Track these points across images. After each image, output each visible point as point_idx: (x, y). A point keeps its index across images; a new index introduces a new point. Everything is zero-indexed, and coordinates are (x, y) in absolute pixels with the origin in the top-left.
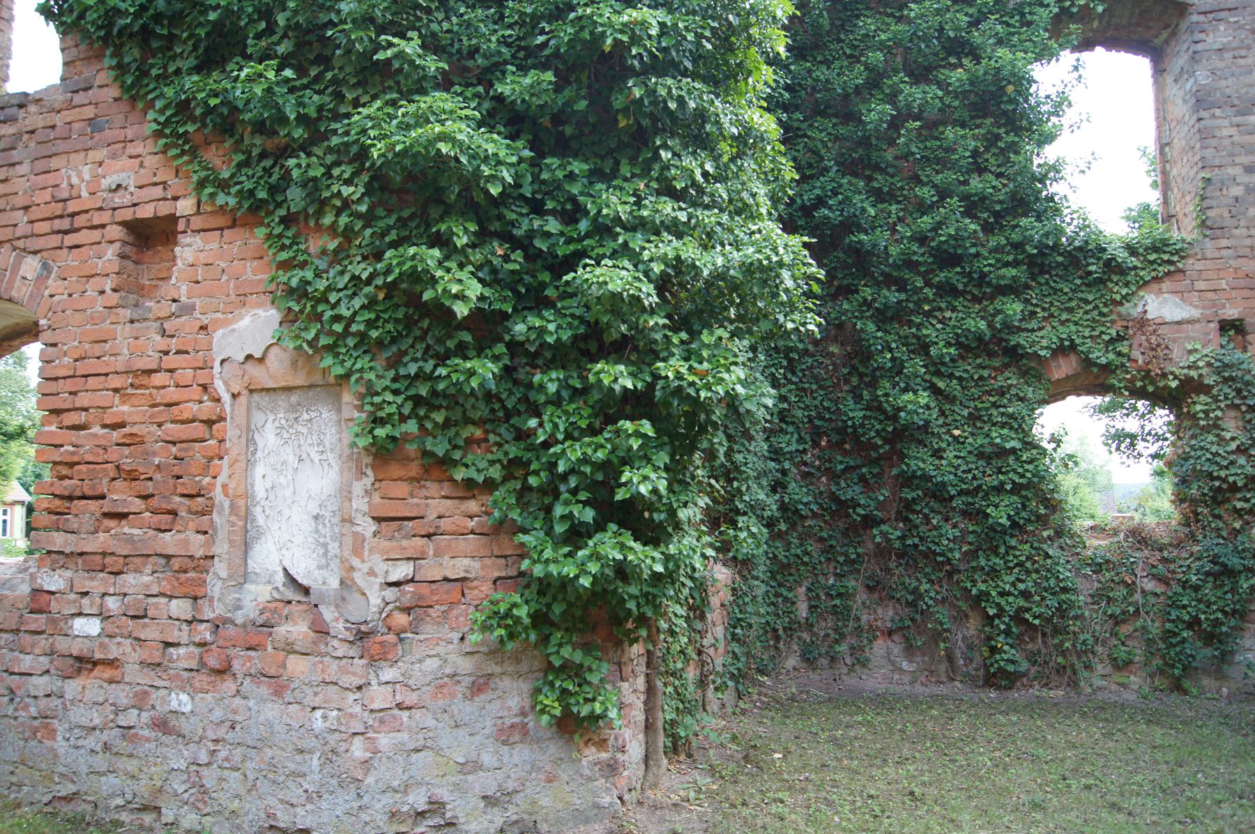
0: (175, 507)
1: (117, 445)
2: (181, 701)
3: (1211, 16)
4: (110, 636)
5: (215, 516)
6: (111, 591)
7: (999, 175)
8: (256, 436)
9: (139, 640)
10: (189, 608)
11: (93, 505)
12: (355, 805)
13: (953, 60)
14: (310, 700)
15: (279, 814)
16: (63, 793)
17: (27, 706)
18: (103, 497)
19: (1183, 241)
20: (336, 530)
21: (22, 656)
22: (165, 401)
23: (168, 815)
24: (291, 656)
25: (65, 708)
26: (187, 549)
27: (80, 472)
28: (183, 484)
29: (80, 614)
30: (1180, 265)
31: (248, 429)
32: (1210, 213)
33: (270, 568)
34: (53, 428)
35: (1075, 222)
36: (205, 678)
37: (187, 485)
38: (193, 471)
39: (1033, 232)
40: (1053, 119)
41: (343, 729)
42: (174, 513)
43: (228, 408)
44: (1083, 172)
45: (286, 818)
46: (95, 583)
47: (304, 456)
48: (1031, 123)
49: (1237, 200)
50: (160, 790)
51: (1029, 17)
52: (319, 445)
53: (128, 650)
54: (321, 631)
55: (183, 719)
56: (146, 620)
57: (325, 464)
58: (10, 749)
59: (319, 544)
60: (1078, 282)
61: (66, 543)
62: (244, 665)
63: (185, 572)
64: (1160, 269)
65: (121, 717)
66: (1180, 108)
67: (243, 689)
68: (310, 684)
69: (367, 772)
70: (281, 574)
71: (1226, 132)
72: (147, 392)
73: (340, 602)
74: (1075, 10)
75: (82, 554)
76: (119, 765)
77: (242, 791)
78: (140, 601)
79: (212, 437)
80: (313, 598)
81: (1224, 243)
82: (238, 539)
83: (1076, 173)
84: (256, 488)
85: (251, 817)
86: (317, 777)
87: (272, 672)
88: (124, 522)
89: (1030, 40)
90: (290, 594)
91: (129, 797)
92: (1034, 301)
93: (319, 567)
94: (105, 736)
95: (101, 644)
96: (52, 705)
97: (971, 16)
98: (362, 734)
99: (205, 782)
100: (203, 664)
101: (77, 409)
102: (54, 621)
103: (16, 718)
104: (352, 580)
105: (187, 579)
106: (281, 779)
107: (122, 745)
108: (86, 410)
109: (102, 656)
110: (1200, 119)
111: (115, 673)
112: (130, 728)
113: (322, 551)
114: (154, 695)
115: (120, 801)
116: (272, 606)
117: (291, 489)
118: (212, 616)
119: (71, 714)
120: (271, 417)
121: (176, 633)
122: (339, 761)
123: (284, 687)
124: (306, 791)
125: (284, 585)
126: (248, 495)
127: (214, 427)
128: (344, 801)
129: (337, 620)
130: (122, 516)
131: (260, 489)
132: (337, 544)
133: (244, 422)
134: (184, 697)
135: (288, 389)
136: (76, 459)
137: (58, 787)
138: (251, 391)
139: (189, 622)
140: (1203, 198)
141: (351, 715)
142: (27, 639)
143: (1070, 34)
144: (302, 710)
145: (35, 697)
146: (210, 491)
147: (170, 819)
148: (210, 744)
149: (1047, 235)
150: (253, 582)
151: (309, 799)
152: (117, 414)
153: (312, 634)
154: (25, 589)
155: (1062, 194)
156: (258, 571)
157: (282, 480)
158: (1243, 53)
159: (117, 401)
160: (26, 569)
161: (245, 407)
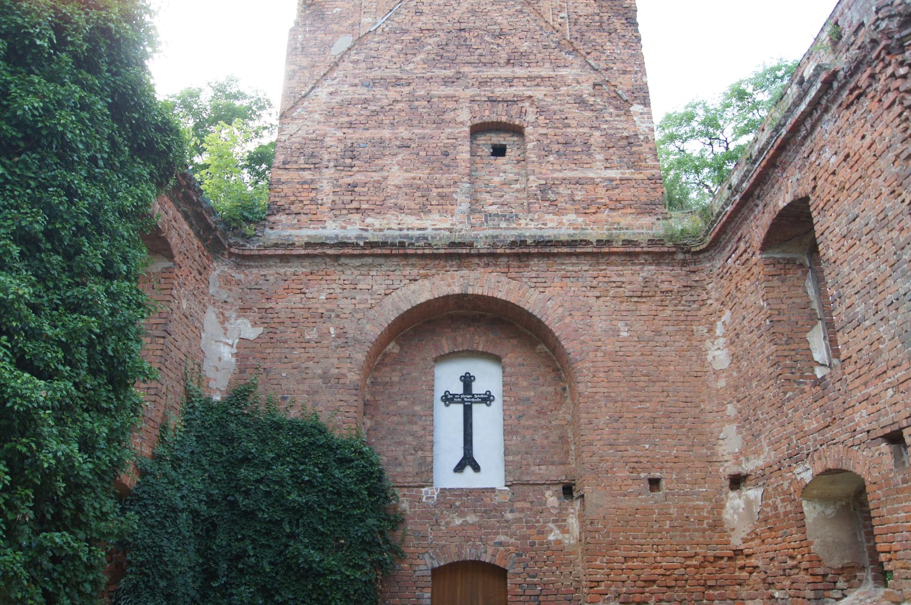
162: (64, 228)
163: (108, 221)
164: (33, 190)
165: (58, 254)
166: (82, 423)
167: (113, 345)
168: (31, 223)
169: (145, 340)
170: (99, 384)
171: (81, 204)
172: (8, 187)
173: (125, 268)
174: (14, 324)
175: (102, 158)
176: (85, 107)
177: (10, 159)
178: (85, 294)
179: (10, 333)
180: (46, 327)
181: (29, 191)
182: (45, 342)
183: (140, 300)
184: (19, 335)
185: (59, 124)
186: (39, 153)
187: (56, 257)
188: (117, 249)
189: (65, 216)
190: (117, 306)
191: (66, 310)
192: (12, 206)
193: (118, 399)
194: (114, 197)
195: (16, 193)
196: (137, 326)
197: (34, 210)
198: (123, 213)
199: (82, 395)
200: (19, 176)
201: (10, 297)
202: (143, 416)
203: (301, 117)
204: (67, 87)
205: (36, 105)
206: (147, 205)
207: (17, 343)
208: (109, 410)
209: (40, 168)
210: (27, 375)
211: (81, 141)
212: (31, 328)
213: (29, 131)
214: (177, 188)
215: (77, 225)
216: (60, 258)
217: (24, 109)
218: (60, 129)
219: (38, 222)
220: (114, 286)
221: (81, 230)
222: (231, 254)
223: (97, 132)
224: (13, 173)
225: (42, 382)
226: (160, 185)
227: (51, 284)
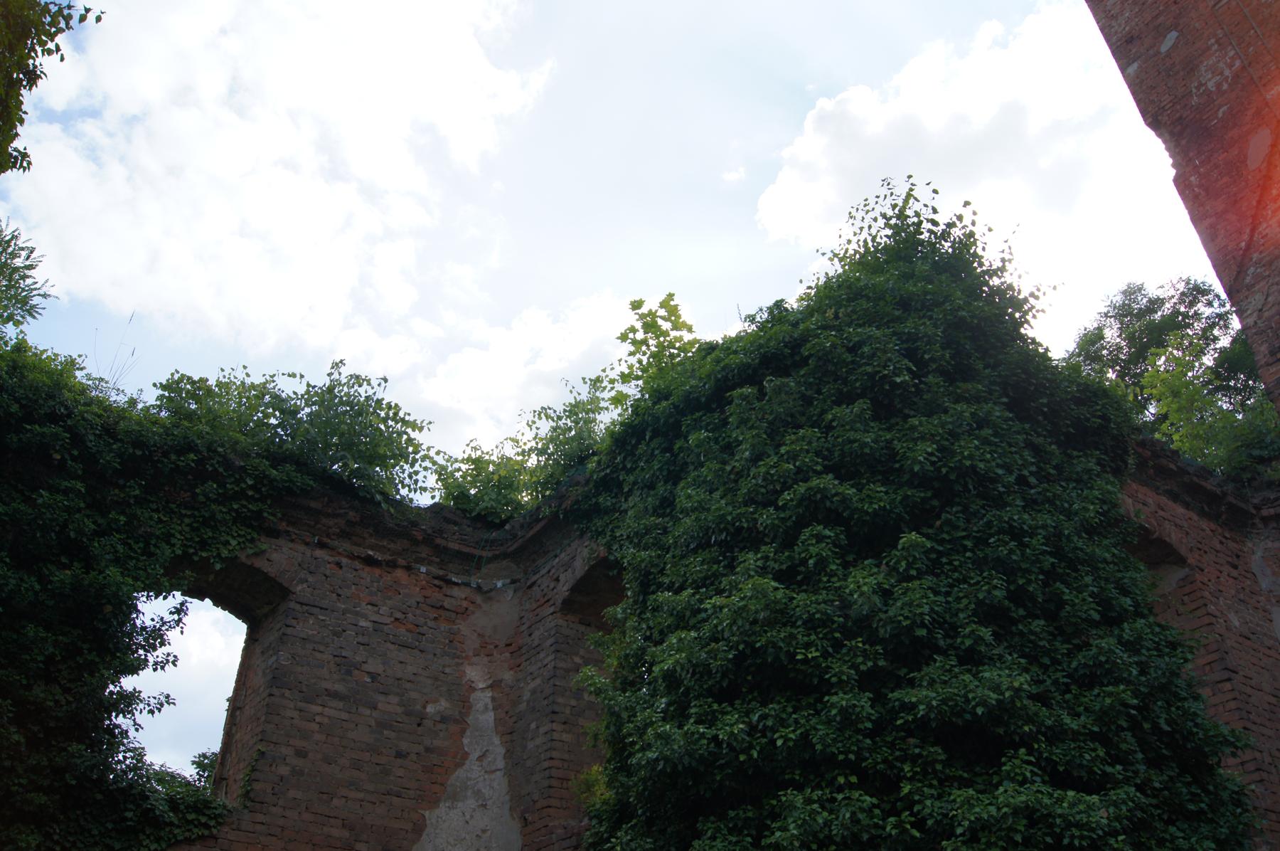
3: (306, 608)
7: (66, 691)
13: (64, 560)
19: (225, 807)
30: (215, 831)
32: (257, 786)
35: (128, 762)
39: (79, 761)
40: (141, 652)
44: (151, 712)
48: (118, 649)
49: (282, 778)
51: (152, 549)
60: (110, 826)
64: (196, 830)
66: (258, 680)
71: (289, 713)
74: (196, 558)
81: (260, 817)
83: (145, 712)
89: (145, 570)
92: (56, 837)
97: (99, 526)
110: (271, 695)
140: (254, 770)
143: (185, 578)
149: (94, 766)
155: (124, 727)
158: (322, 648)
162: (1029, 582)
163: (1077, 548)
164: (972, 551)
165: (1038, 617)
166: (1172, 841)
167: (1164, 716)
168: (989, 592)
169: (1205, 692)
170: (1171, 778)
171: (1034, 542)
172: (944, 560)
173: (1129, 601)
174: (1026, 728)
175: (1031, 473)
176: (982, 423)
177: (931, 526)
178: (1095, 657)
179: (1026, 741)
180: (1067, 720)
181: (968, 554)
182: (1073, 740)
183: (1170, 638)
184: (1038, 741)
185: (964, 458)
186: (959, 504)
187: (1037, 622)
188: (1107, 580)
189: (1024, 566)
190: (1143, 659)
191: (1080, 687)
192: (958, 580)
193: (1208, 792)
194: (1069, 515)
195: (956, 563)
196: (1184, 676)
197: (985, 574)
198: (1090, 531)
199: (1154, 801)
200: (949, 541)
201: (1007, 694)
202: (1255, 808)
203: (1258, 278)
204: (951, 411)
205: (929, 450)
206: (1115, 506)
207: (1041, 753)
208: (1202, 812)
209: (968, 521)
210: (1071, 793)
211: (998, 466)
212: (1048, 728)
213: (936, 484)
214: (1142, 464)
215: (1042, 572)
216: (1042, 622)
217: (920, 462)
218: (968, 463)
219: (995, 587)
220: (1127, 631)
221: (1051, 576)
222: (1266, 520)
223: (1011, 446)
224: (942, 542)
225: (1095, 798)
226: (1117, 472)
227: (1046, 661)
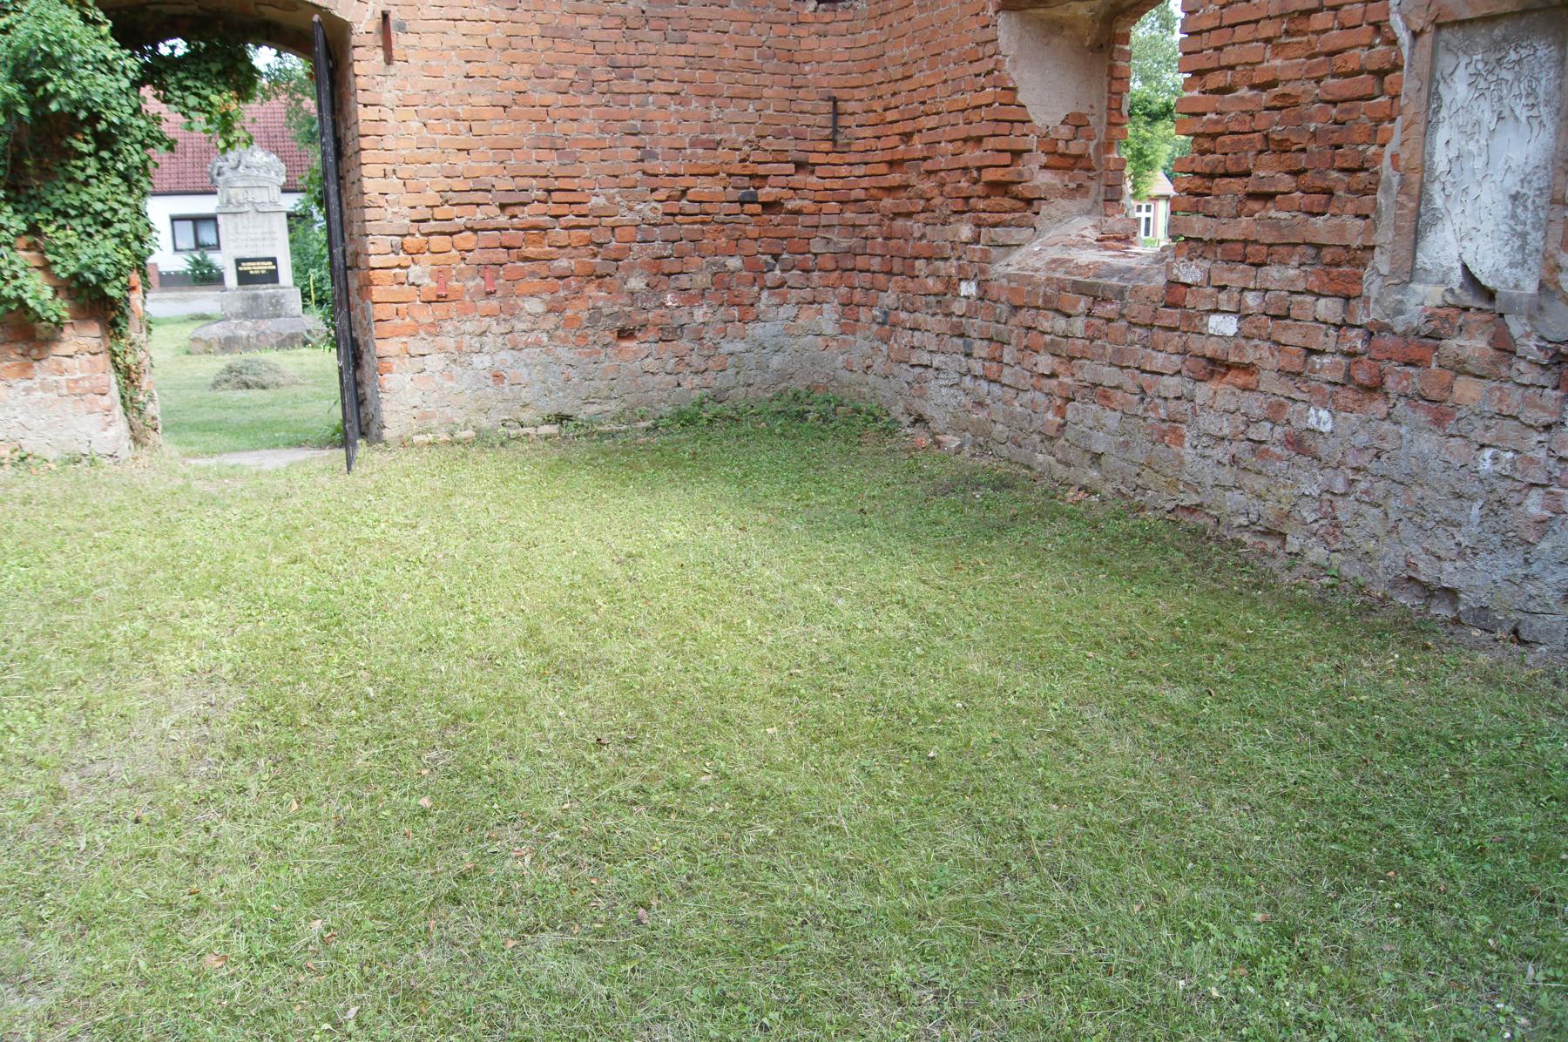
0: (1331, 184)
1: (1267, 109)
2: (1320, 418)
4: (1247, 338)
5: (1380, 196)
6: (1252, 286)
8: (1442, 88)
9: (1277, 343)
10: (1339, 310)
11: (1236, 184)
12: (1520, 572)
14: (1478, 435)
15: (1421, 565)
16: (1186, 503)
17: (1156, 408)
18: (1248, 174)
20: (1542, 215)
21: (1154, 354)
22: (1325, 50)
23: (1294, 544)
24: (1460, 378)
25: (1195, 414)
26: (1342, 237)
27: (1223, 144)
28: (1343, 155)
29: (1216, 311)
31: (1432, 79)
33: (1445, 263)
34: (1195, 93)
36: (1351, 395)
37: (1347, 157)
38: (1356, 137)
41: (1518, 476)
42: (1329, 192)
43: (1405, 52)
45: (1430, 572)
46: (1234, 276)
47: (1506, 113)
50: (1288, 515)
52: (1528, 95)
53: (1266, 354)
54: (1505, 348)
55: (1320, 439)
56: (1288, 322)
57: (1535, 123)
58: (1138, 450)
59: (1514, 233)
61: (1205, 229)
62: (1399, 383)
63: (1338, 265)
65: (1252, 429)
67: (1395, 412)
68: (1481, 416)
69: (1542, 535)
70: (1459, 272)
72: (1305, 39)
73: (1536, 310)
75: (1221, 242)
76: (1246, 481)
77: (1380, 532)
78: (1283, 299)
79: (1382, 93)
80: (1498, 306)
82: (1407, 225)
84: (1436, 159)
85: (1387, 562)
86: (1475, 530)
87: (1434, 395)
88: (1270, 204)
90: (1468, 299)
91: (1253, 517)
93: (1512, 265)
94: (1234, 448)
95: (1237, 346)
96: (1181, 409)
98: (1543, 486)
99: (1338, 514)
100: (1349, 377)
101: (1221, 68)
102: (1188, 317)
103: (1145, 419)
104: (1557, 284)
105: (1340, 274)
106: (1429, 525)
107: (1251, 461)
108: (1232, 68)
109: (1236, 359)
111: (1251, 380)
112: (1261, 442)
113: (1518, 243)
114: (1291, 409)
115: (1243, 520)
116: (1443, 312)
117: (1484, 158)
118: (1365, 320)
119: (1200, 420)
120: (1464, 60)
121: (1322, 338)
122: (1507, 515)
123: (1449, 415)
124: (1458, 544)
125: (1461, 286)
126: (1425, 168)
127: (1387, 79)
128: (1507, 564)
129: (1528, 335)
130: (1267, 197)
131: (1441, 160)
132: (1540, 234)
133: (1426, 70)
134: (1324, 414)
135: (1490, 19)
136: (1219, 129)
137: (1182, 496)
138: (1439, 27)
139: (1338, 327)
141: (1532, 461)
142: (1160, 335)
144: (1466, 446)
145: (1166, 399)
146: (1376, 164)
147: (1295, 549)
148: (1349, 472)
150: (1421, 281)
151: (1461, 555)
152: (1263, 70)
153: (1491, 352)
154: (1161, 280)
156: (1428, 266)
157: (1472, 146)
159: (1268, 55)
160: (1163, 260)
161: (1428, 48)
